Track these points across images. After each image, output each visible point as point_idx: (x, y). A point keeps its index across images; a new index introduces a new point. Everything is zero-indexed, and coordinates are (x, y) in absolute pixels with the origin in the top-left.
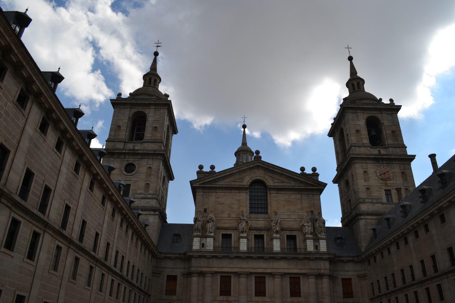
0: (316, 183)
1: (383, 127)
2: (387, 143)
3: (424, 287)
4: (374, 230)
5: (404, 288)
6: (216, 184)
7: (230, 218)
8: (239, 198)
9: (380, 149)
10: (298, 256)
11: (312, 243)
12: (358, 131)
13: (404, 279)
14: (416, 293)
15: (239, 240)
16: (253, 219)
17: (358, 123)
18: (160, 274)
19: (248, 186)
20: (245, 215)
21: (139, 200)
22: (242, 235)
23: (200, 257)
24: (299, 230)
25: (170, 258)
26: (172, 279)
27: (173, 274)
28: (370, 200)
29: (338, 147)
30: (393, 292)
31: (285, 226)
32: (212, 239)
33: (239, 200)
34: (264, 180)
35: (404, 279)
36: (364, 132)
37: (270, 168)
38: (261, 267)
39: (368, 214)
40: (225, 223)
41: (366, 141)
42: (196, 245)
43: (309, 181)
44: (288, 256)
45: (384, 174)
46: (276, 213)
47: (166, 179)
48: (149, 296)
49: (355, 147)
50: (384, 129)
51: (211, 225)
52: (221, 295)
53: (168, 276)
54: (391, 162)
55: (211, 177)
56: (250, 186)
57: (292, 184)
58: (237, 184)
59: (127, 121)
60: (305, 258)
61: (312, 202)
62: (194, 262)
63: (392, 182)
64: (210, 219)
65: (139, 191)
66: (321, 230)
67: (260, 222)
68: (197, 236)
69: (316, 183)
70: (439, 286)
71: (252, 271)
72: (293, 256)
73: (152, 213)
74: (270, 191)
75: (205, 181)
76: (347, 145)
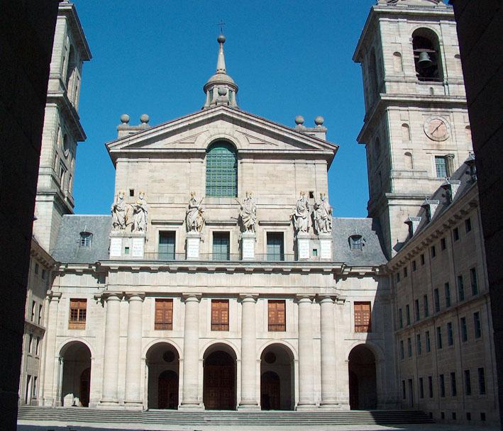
0: (319, 145)
1: (441, 47)
2: (445, 75)
3: (460, 317)
4: (409, 223)
5: (437, 317)
6: (150, 146)
7: (173, 205)
8: (188, 172)
9: (431, 86)
10: (282, 267)
11: (308, 245)
12: (397, 54)
13: (437, 304)
14: (450, 324)
15: (186, 241)
16: (212, 206)
17: (399, 40)
18: (59, 298)
19: (205, 151)
20: (198, 199)
22: (192, 232)
23: (121, 269)
24: (289, 225)
25: (73, 272)
28: (410, 174)
29: (368, 80)
30: (424, 323)
31: (266, 217)
33: (189, 175)
34: (232, 139)
35: (437, 304)
36: (409, 56)
37: (243, 119)
38: (221, 283)
39: (404, 198)
40: (164, 214)
41: (411, 72)
42: (116, 251)
44: (266, 266)
45: (437, 128)
47: (70, 140)
49: (390, 82)
50: (442, 51)
51: (140, 218)
52: (156, 329)
53: (72, 300)
54: (450, 110)
56: (208, 150)
57: (282, 146)
58: (185, 147)
60: (294, 271)
63: (447, 142)
64: (138, 207)
68: (118, 236)
69: (322, 146)
70: (476, 315)
72: (274, 267)
74: (241, 159)
75: (131, 143)
76: (379, 79)
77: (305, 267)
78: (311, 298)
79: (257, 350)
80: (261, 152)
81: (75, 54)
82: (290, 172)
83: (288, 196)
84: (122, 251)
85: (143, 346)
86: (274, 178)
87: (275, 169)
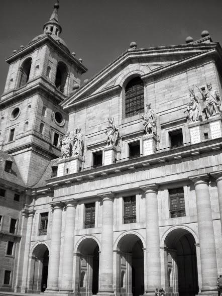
0: (203, 49)
7: (101, 132)
16: (126, 125)
21: (19, 140)
26: (44, 215)
27: (45, 212)
31: (167, 119)
32: (76, 161)
37: (143, 55)
43: (193, 49)
46: (149, 105)
48: (18, 239)
53: (41, 214)
55: (80, 93)
57: (175, 63)
59: (17, 72)
61: (203, 75)
62: (57, 193)
65: (20, 133)
66: (212, 108)
67: (135, 125)
71: (116, 189)
73: (27, 149)
75: (74, 99)
77: (192, 150)
78: (202, 178)
79: (161, 237)
80: (158, 72)
81: (69, 67)
82: (183, 79)
83: (183, 98)
84: (64, 172)
85: (75, 242)
86: (170, 89)
87: (171, 82)
